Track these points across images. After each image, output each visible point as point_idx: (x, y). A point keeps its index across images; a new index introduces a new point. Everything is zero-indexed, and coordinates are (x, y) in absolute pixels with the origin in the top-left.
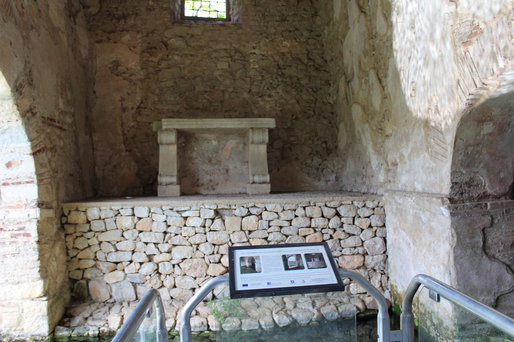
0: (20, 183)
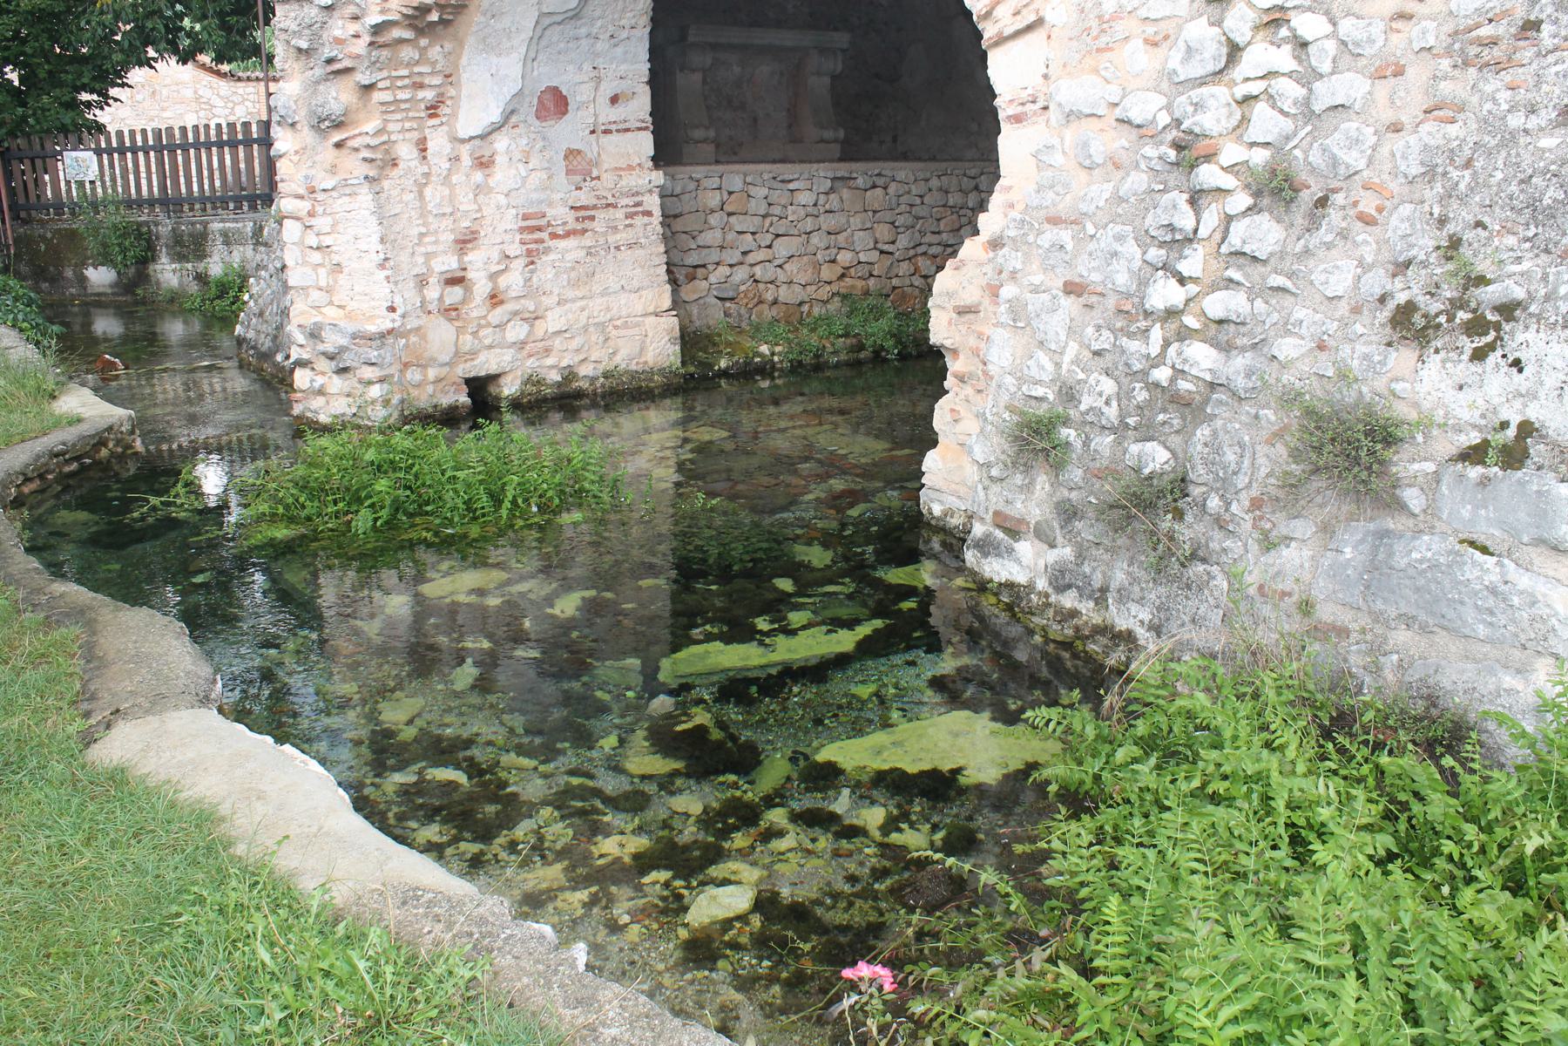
0: (628, 130)
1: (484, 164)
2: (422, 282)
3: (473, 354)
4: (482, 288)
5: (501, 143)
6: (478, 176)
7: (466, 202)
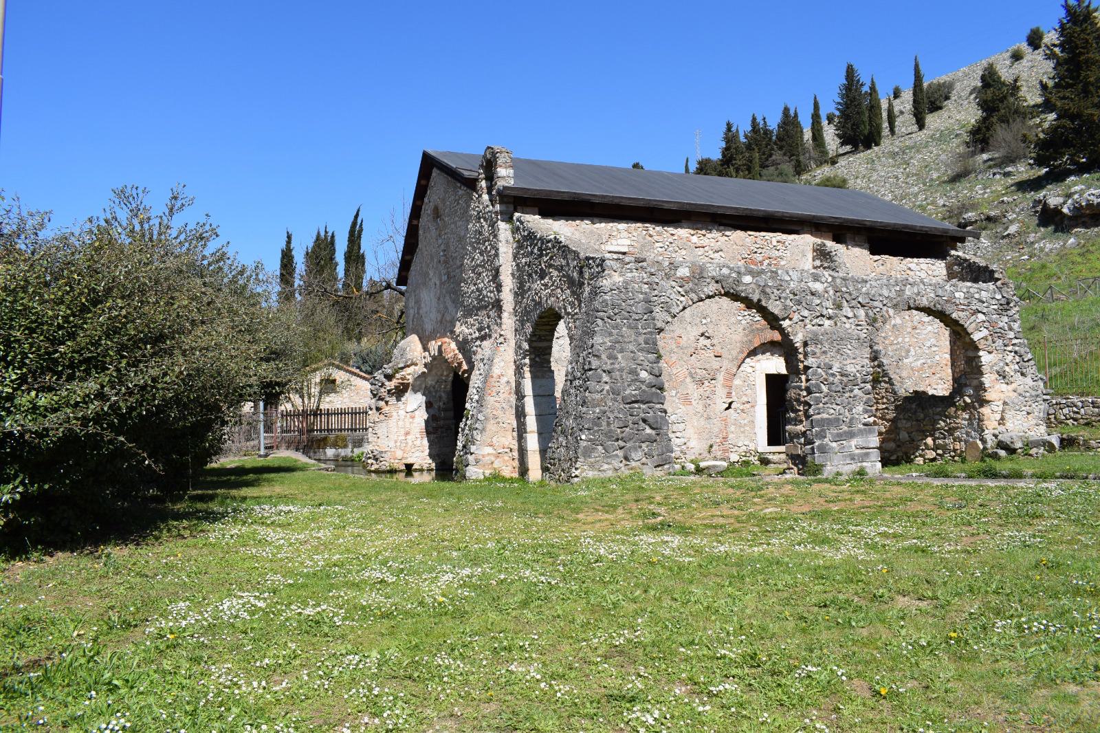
1: (413, 418)
2: (396, 442)
3: (407, 458)
4: (410, 443)
5: (416, 413)
6: (411, 420)
7: (408, 425)
